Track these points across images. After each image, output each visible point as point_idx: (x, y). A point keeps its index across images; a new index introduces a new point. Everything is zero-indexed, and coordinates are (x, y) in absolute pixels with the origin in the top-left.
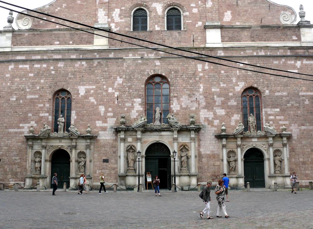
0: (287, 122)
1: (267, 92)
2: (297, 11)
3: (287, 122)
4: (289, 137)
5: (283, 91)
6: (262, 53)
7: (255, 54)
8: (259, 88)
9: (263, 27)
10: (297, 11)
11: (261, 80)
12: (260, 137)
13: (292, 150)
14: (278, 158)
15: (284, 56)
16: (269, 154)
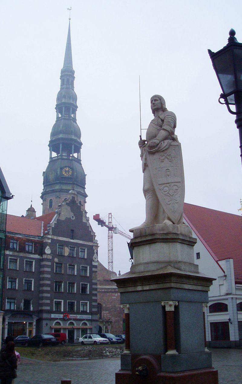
0: (111, 317)
1: (104, 305)
2: (118, 273)
3: (111, 317)
4: (111, 322)
5: (110, 305)
6: (103, 290)
7: (101, 291)
8: (102, 303)
9: (104, 280)
10: (118, 273)
11: (102, 301)
12: (100, 322)
13: (112, 327)
14: (107, 329)
15: (111, 292)
16: (103, 328)
